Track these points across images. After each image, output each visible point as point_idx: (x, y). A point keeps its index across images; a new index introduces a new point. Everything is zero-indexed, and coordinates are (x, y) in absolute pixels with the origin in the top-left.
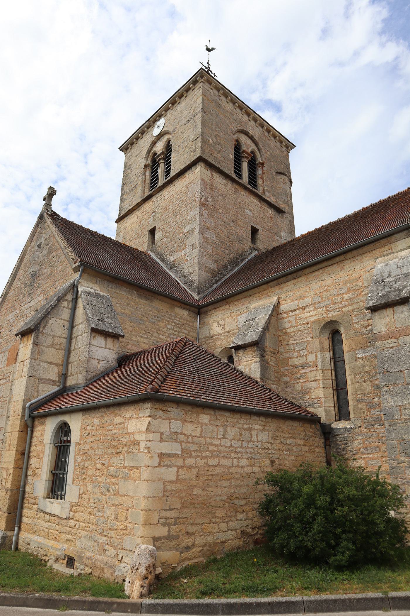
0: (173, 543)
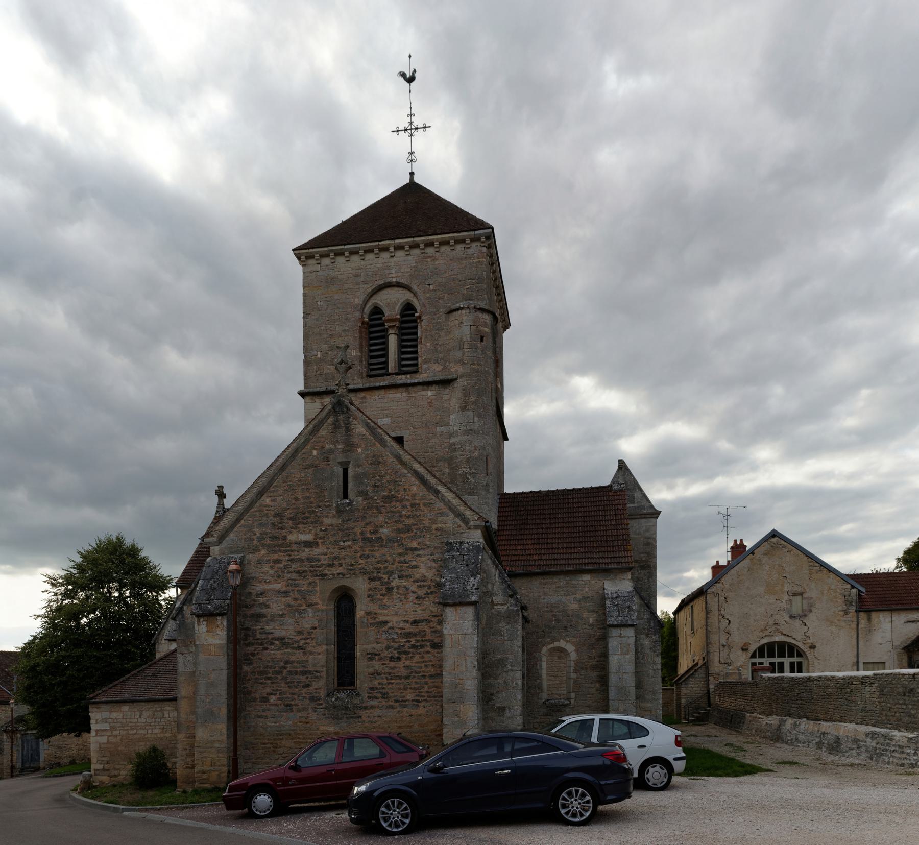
0: (106, 772)
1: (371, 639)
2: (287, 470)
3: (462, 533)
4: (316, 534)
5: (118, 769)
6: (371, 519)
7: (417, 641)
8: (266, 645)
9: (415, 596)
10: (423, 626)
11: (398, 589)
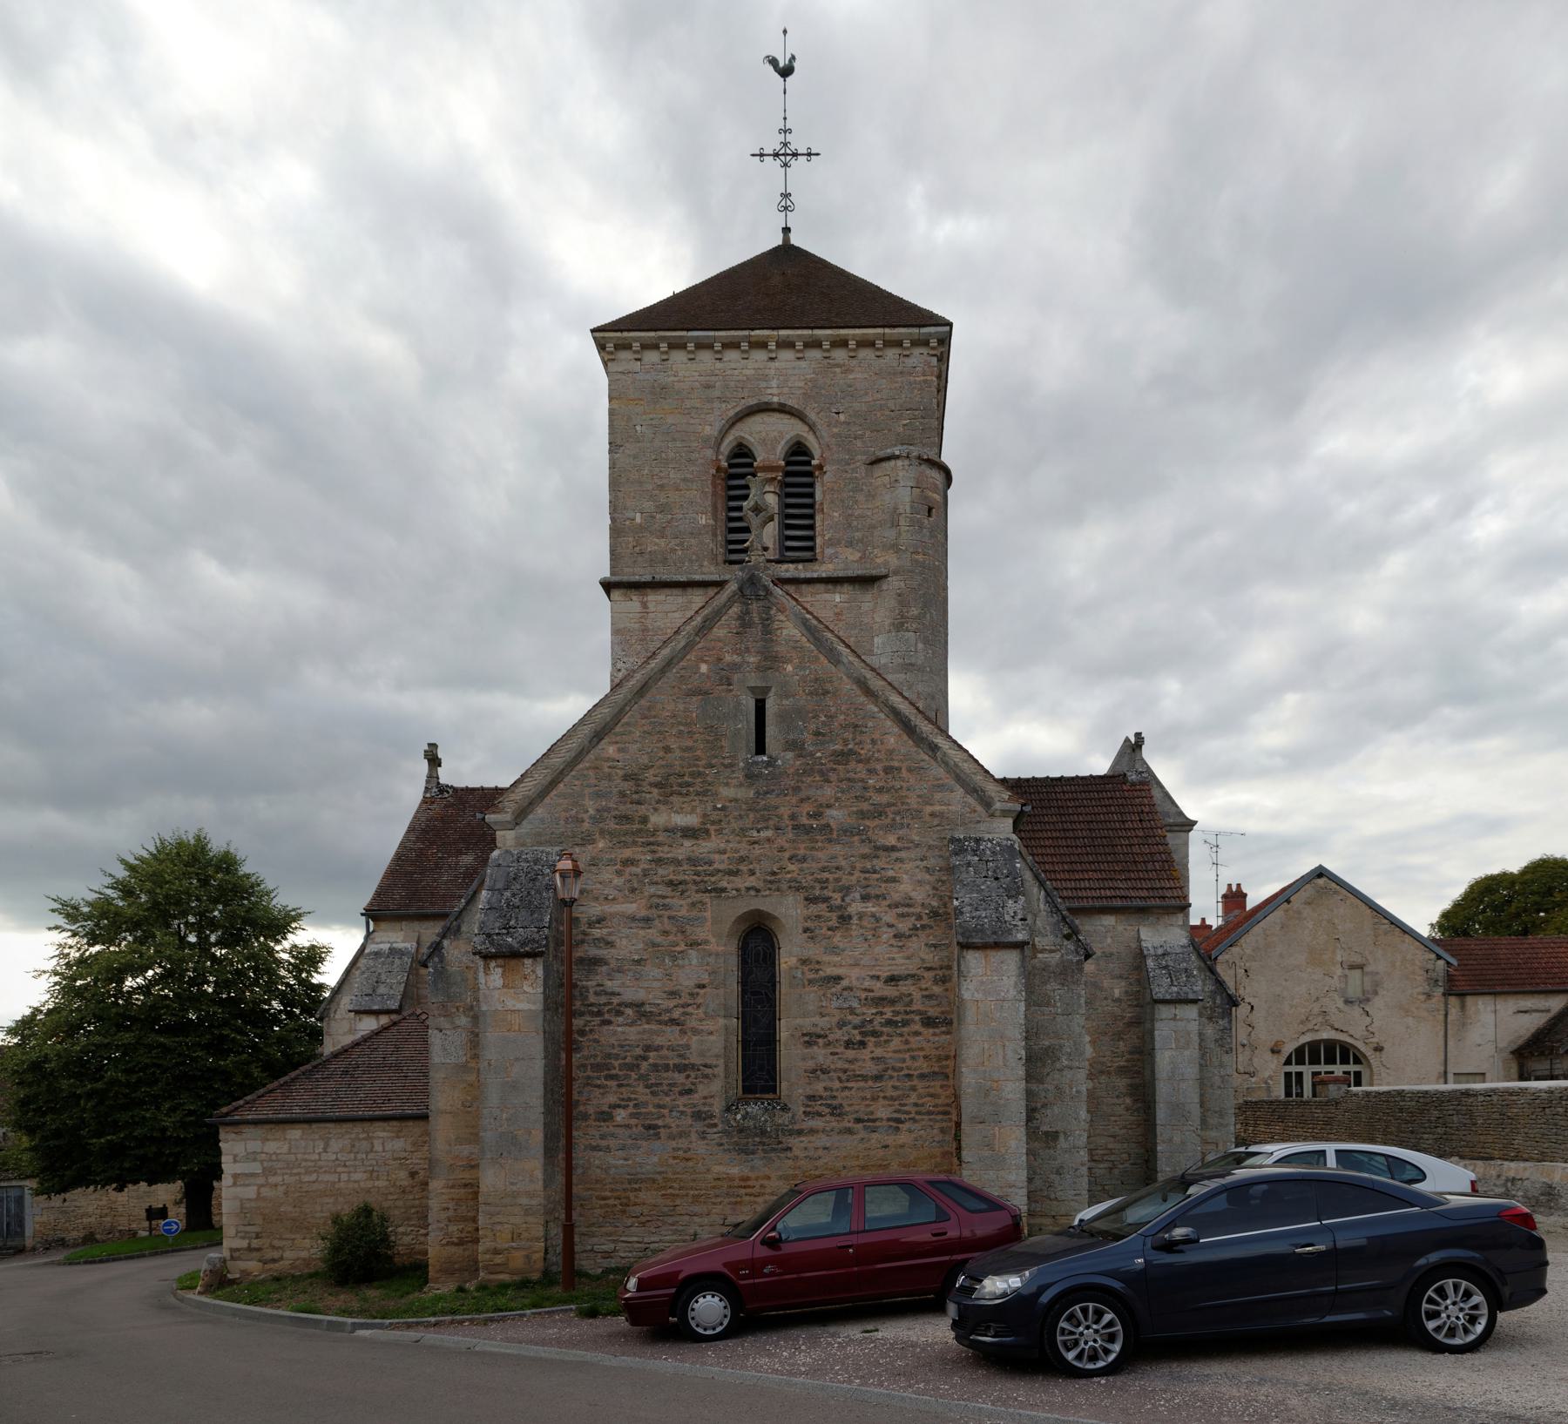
0: (255, 1254)
1: (811, 1008)
2: (648, 696)
3: (979, 822)
4: (705, 815)
5: (278, 1248)
6: (811, 792)
7: (897, 1013)
8: (607, 1016)
9: (892, 931)
10: (906, 987)
11: (860, 918)
